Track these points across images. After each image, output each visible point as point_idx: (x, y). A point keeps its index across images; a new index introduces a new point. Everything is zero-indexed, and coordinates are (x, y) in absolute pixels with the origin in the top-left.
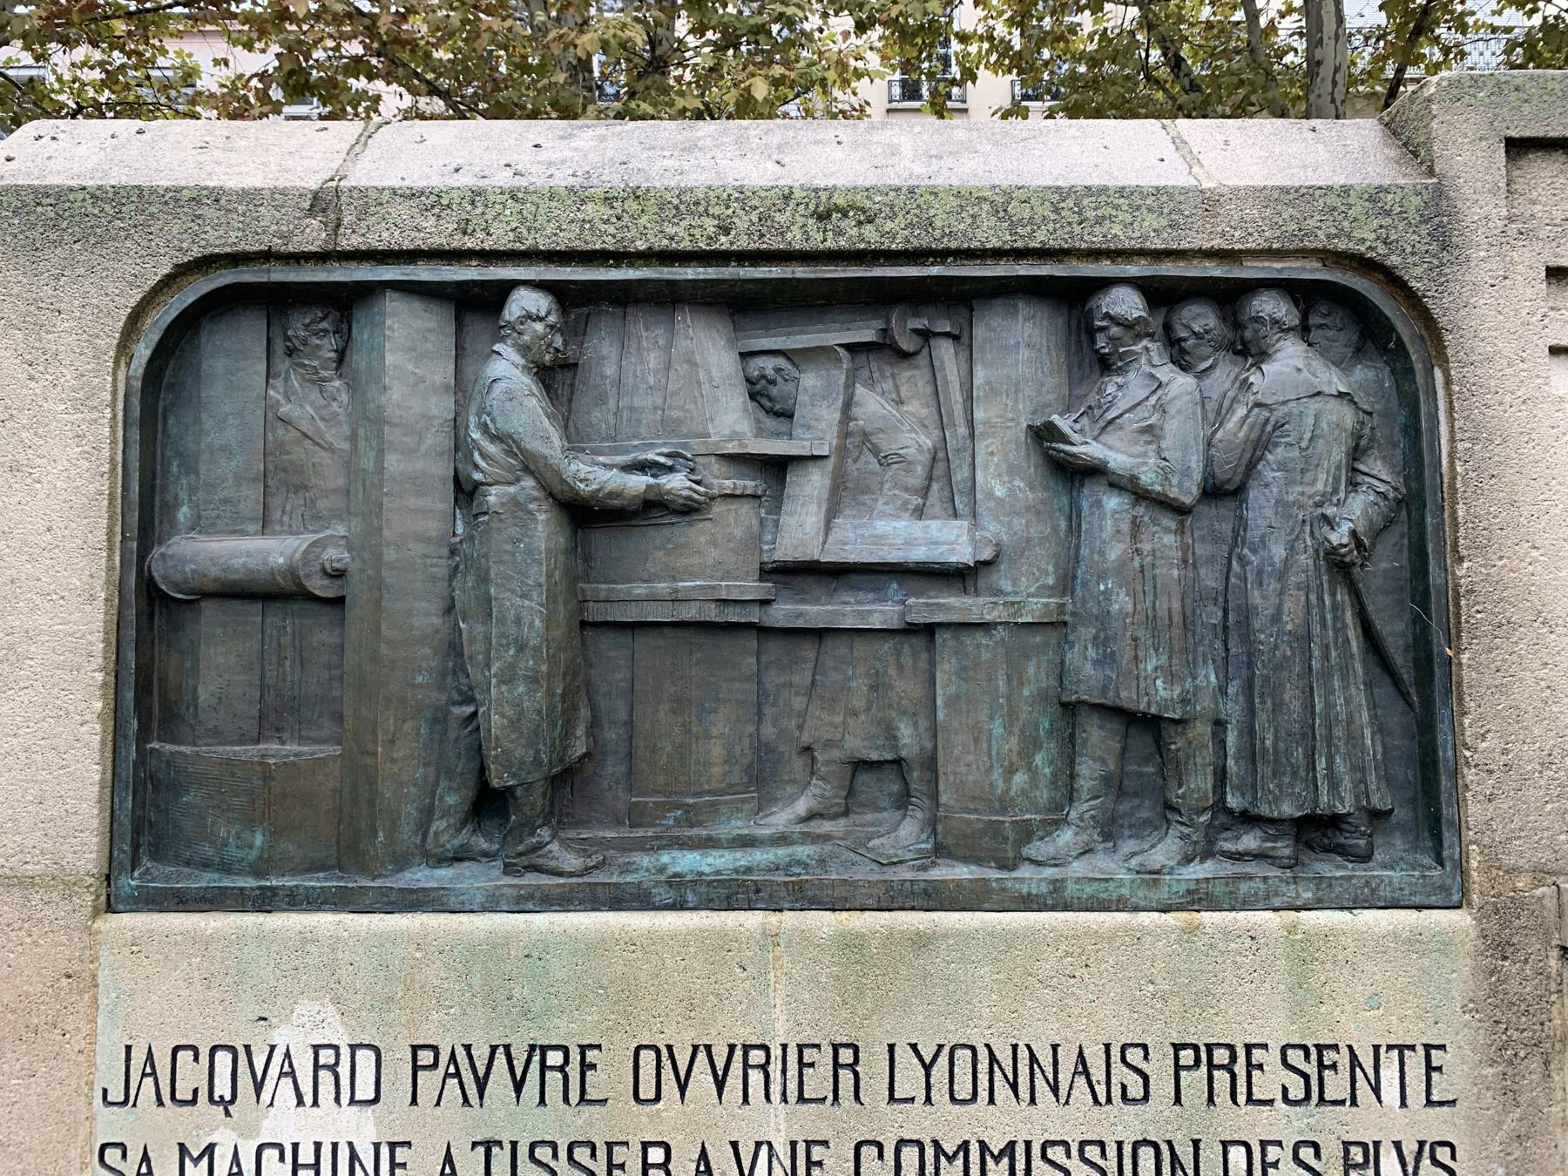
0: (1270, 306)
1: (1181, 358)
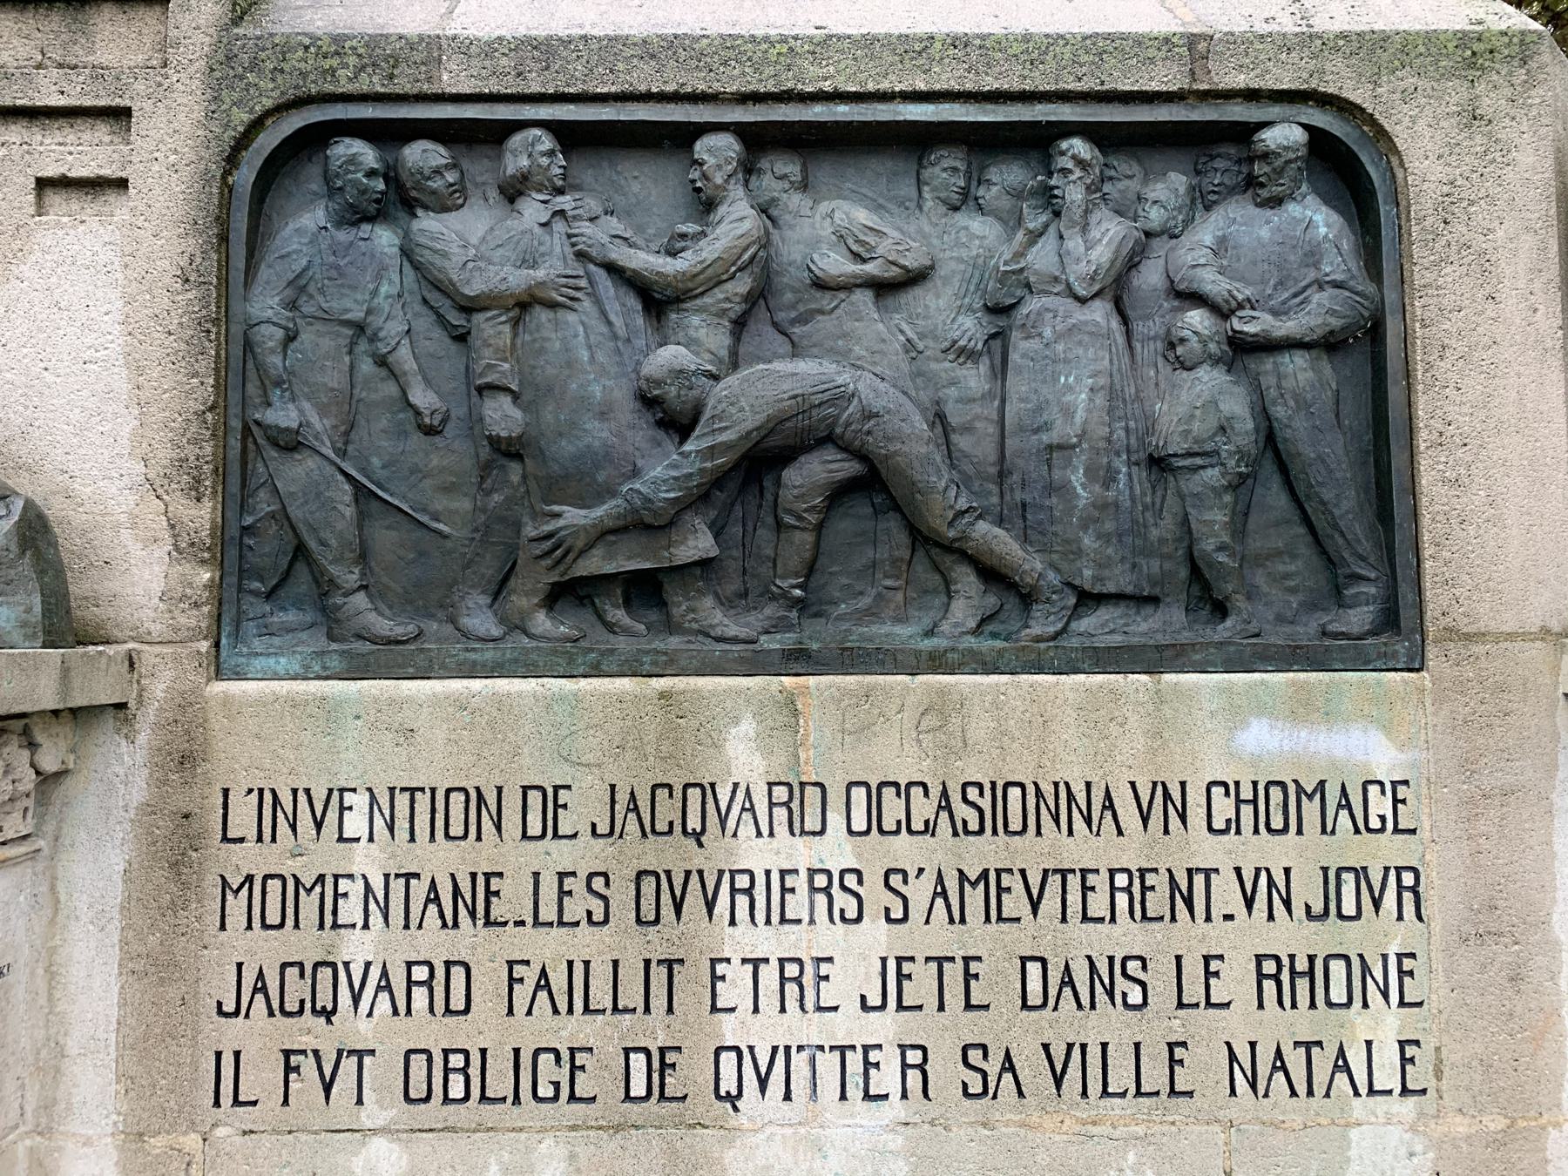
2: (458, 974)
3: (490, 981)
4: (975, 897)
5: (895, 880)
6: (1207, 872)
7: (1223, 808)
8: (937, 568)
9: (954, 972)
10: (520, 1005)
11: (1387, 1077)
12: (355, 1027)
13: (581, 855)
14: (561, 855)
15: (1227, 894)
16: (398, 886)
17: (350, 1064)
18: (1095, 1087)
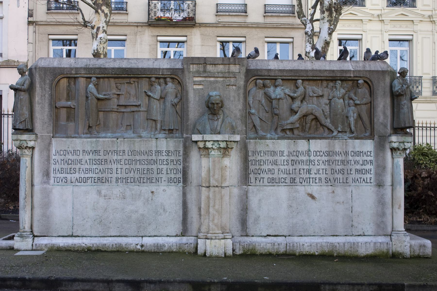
0: (168, 79)
1: (160, 85)
2: (273, 170)
3: (276, 171)
4: (327, 163)
5: (318, 161)
6: (351, 160)
7: (352, 154)
8: (323, 128)
9: (324, 170)
10: (280, 174)
11: (368, 181)
12: (262, 175)
13: (285, 158)
14: (283, 158)
15: (353, 163)
16: (267, 161)
17: (262, 179)
18: (339, 182)
